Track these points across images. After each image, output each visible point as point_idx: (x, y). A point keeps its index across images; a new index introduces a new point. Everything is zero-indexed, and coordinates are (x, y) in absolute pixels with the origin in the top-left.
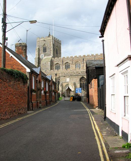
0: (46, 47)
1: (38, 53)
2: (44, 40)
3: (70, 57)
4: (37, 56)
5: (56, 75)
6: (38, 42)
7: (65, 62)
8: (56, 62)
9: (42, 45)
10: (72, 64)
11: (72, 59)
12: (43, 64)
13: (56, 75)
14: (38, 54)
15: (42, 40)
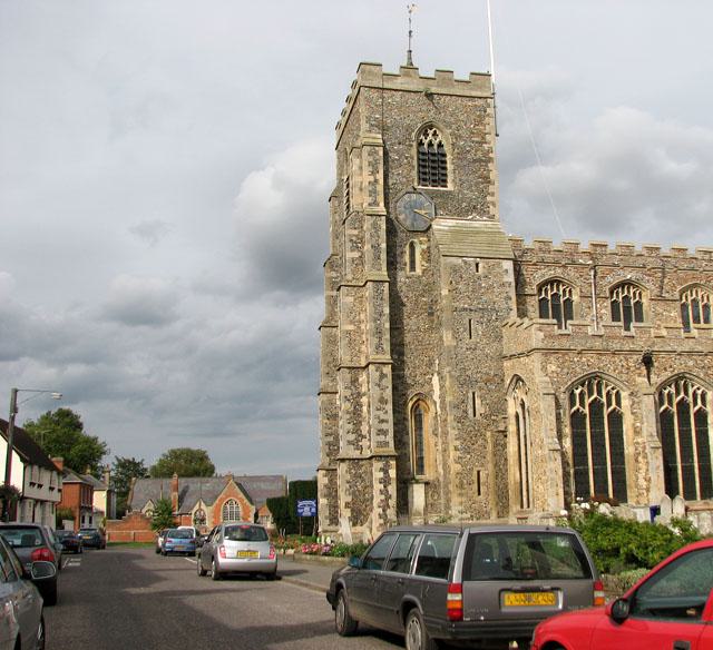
0: (440, 145)
1: (380, 176)
2: (429, 96)
3: (638, 249)
4: (375, 203)
5: (648, 361)
6: (375, 94)
7: (612, 280)
8: (549, 273)
9: (409, 129)
10: (659, 298)
11: (662, 265)
12: (455, 270)
13: (648, 361)
14: (380, 187)
15: (406, 87)
